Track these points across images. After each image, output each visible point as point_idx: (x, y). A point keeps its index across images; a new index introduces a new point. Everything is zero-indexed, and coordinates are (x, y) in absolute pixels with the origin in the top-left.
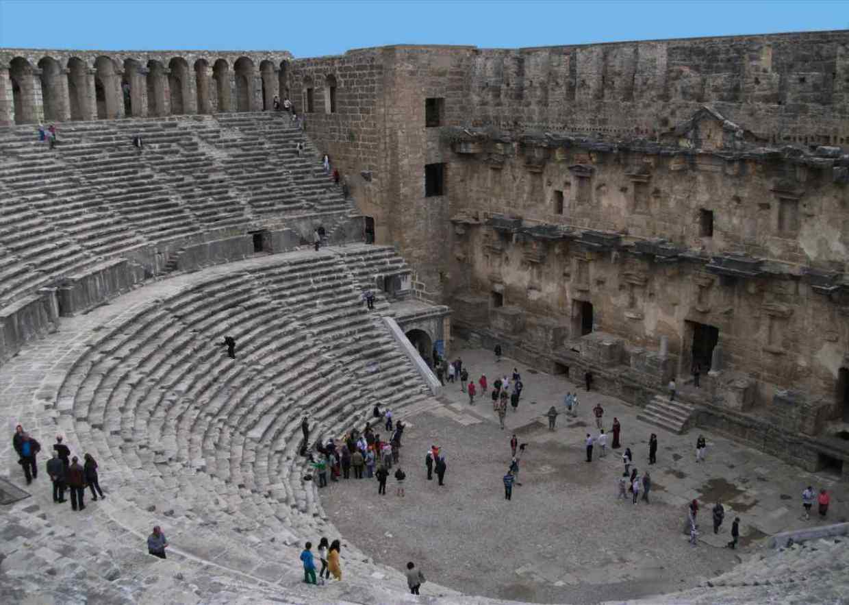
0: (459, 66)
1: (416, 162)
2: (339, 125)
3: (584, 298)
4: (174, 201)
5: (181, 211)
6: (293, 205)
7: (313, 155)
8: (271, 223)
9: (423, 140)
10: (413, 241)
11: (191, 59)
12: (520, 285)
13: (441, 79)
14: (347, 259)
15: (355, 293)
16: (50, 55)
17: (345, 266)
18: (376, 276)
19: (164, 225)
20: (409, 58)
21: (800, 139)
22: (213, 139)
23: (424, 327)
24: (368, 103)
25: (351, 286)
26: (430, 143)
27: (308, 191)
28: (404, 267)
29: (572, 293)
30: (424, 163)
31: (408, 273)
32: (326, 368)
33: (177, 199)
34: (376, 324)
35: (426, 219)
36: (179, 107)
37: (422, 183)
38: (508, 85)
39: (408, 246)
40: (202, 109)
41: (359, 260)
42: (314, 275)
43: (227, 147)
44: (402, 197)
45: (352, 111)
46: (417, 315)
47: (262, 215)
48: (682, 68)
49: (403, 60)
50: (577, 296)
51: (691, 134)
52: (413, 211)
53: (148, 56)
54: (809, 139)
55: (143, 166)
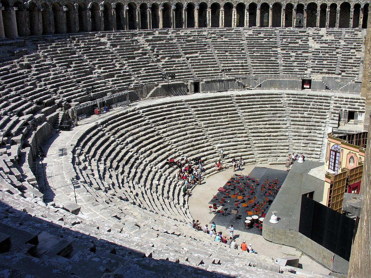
4: (278, 62)
5: (278, 66)
6: (330, 72)
7: (361, 51)
8: (316, 78)
11: (319, 3)
14: (337, 99)
16: (255, 2)
18: (344, 109)
19: (264, 70)
22: (318, 38)
25: (327, 111)
31: (364, 112)
33: (280, 61)
34: (323, 128)
36: (311, 24)
40: (322, 25)
41: (341, 101)
42: (314, 102)
43: (321, 43)
46: (349, 131)
47: (313, 73)
53: (298, 2)
55: (276, 47)
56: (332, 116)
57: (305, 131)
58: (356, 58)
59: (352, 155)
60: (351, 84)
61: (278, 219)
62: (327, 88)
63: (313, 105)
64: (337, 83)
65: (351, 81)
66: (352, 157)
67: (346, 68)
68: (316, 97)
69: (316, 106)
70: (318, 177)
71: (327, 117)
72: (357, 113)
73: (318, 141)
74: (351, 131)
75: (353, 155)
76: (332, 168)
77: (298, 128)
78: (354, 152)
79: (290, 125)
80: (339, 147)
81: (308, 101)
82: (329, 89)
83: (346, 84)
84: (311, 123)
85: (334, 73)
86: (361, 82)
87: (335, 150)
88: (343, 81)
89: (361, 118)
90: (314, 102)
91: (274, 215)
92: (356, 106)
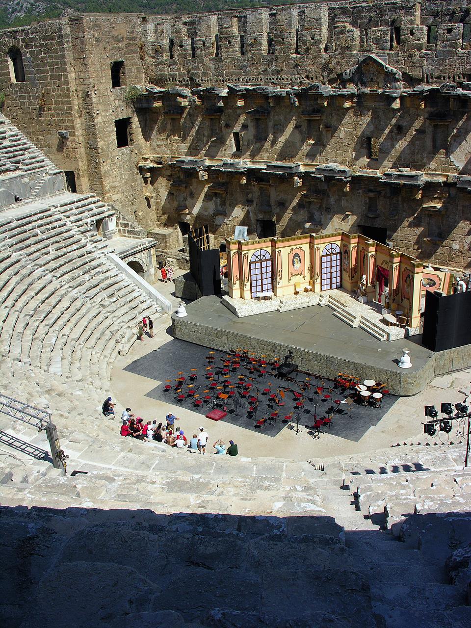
0: (133, 32)
1: (107, 119)
2: (28, 92)
3: (267, 218)
9: (112, 99)
10: (111, 187)
12: (206, 214)
13: (122, 45)
15: (77, 237)
17: (62, 216)
18: (89, 220)
20: (95, 26)
21: (449, 78)
23: (137, 258)
24: (58, 70)
25: (72, 233)
26: (116, 101)
27: (11, 154)
28: (109, 210)
29: (256, 214)
30: (114, 119)
31: (113, 214)
32: (77, 304)
34: (103, 260)
35: (120, 167)
37: (114, 136)
38: (181, 46)
39: (108, 193)
44: (100, 151)
45: (41, 78)
46: (132, 249)
48: (346, 24)
49: (89, 28)
50: (260, 216)
51: (356, 79)
52: (109, 161)
54: (456, 77)
56: (89, 237)
57: (87, 277)
58: (13, 136)
59: (295, 252)
60: (49, 179)
61: (397, 362)
62: (17, 200)
63: (43, 232)
64: (26, 185)
65: (44, 174)
66: (297, 255)
67: (16, 157)
68: (34, 218)
69: (47, 232)
70: (257, 311)
71: (83, 241)
72: (107, 218)
73: (117, 283)
74: (135, 248)
75: (297, 251)
76: (259, 288)
77: (73, 279)
78: (298, 247)
79: (57, 278)
80: (263, 253)
81: (30, 230)
82: (21, 200)
83: (40, 183)
84: (74, 261)
85: (8, 170)
86: (61, 172)
87: (257, 260)
88: (33, 179)
89: (112, 225)
90: (40, 226)
91: (407, 355)
92: (95, 211)
